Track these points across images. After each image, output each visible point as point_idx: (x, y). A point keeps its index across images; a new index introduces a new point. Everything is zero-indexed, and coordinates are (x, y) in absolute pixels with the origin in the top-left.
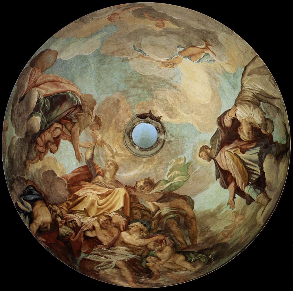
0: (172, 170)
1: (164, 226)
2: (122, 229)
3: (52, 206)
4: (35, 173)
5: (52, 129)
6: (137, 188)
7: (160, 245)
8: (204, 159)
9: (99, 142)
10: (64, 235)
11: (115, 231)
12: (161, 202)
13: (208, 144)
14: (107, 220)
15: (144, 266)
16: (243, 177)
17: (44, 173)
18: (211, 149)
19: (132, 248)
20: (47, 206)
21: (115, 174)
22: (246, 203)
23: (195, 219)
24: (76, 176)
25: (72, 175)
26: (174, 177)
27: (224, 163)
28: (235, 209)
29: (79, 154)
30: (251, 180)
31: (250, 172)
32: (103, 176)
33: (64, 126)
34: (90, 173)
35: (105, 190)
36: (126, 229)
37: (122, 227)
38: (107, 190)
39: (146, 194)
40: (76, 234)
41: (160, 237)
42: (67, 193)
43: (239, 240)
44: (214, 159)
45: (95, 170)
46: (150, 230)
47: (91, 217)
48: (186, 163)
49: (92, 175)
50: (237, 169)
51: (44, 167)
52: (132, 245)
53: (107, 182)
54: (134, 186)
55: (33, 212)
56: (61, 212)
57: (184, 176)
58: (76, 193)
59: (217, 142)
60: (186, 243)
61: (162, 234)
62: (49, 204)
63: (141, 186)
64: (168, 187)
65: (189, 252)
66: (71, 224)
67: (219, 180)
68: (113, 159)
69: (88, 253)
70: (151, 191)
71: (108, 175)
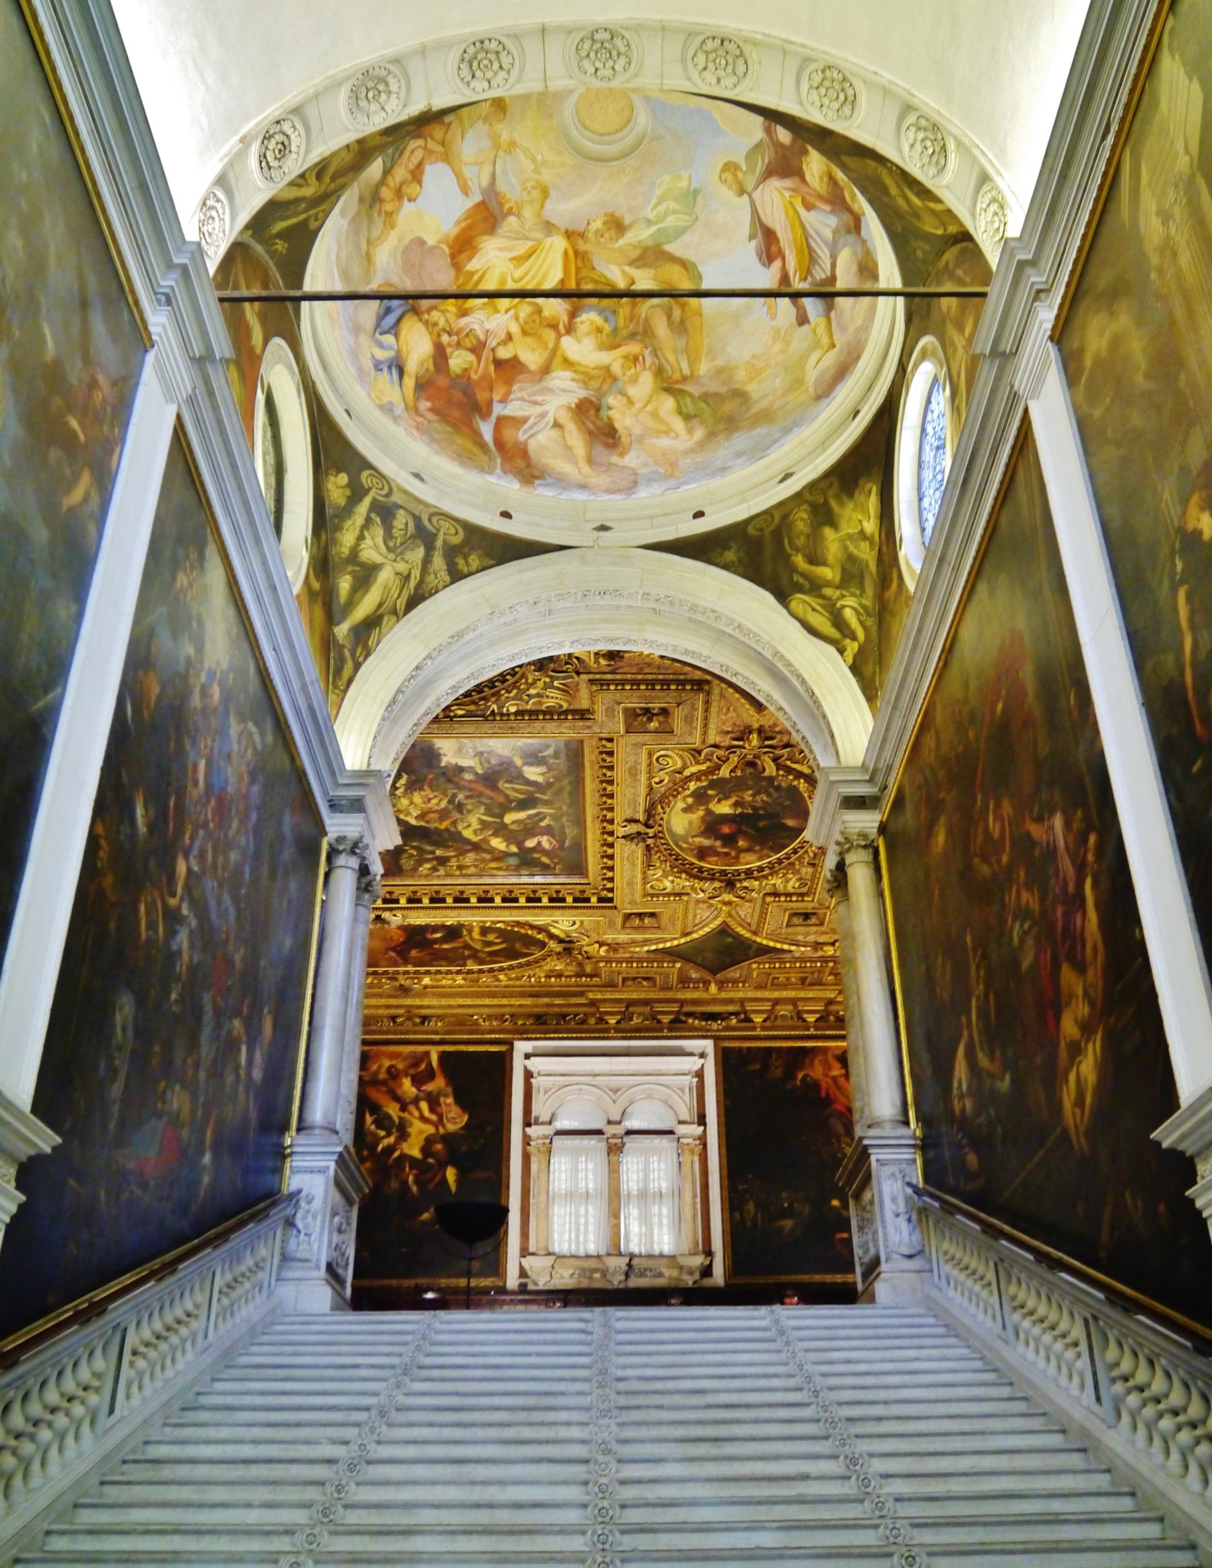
0: (661, 200)
1: (642, 321)
2: (563, 331)
5: (407, 154)
8: (730, 188)
10: (459, 371)
11: (550, 335)
12: (638, 267)
13: (740, 159)
14: (533, 313)
15: (605, 419)
16: (800, 261)
20: (421, 320)
21: (542, 206)
24: (463, 231)
25: (456, 230)
26: (666, 215)
28: (774, 323)
29: (465, 182)
30: (812, 276)
31: (810, 258)
32: (519, 215)
33: (429, 140)
35: (523, 247)
36: (570, 330)
37: (561, 327)
38: (530, 244)
40: (479, 362)
41: (634, 348)
42: (452, 272)
44: (750, 195)
45: (501, 205)
46: (615, 331)
47: (503, 311)
49: (495, 218)
50: (791, 237)
51: (401, 238)
53: (527, 227)
56: (447, 321)
58: (470, 267)
59: (760, 163)
60: (681, 369)
62: (422, 313)
63: (598, 231)
64: (653, 235)
67: (754, 242)
69: (504, 401)
70: (617, 240)
71: (528, 212)
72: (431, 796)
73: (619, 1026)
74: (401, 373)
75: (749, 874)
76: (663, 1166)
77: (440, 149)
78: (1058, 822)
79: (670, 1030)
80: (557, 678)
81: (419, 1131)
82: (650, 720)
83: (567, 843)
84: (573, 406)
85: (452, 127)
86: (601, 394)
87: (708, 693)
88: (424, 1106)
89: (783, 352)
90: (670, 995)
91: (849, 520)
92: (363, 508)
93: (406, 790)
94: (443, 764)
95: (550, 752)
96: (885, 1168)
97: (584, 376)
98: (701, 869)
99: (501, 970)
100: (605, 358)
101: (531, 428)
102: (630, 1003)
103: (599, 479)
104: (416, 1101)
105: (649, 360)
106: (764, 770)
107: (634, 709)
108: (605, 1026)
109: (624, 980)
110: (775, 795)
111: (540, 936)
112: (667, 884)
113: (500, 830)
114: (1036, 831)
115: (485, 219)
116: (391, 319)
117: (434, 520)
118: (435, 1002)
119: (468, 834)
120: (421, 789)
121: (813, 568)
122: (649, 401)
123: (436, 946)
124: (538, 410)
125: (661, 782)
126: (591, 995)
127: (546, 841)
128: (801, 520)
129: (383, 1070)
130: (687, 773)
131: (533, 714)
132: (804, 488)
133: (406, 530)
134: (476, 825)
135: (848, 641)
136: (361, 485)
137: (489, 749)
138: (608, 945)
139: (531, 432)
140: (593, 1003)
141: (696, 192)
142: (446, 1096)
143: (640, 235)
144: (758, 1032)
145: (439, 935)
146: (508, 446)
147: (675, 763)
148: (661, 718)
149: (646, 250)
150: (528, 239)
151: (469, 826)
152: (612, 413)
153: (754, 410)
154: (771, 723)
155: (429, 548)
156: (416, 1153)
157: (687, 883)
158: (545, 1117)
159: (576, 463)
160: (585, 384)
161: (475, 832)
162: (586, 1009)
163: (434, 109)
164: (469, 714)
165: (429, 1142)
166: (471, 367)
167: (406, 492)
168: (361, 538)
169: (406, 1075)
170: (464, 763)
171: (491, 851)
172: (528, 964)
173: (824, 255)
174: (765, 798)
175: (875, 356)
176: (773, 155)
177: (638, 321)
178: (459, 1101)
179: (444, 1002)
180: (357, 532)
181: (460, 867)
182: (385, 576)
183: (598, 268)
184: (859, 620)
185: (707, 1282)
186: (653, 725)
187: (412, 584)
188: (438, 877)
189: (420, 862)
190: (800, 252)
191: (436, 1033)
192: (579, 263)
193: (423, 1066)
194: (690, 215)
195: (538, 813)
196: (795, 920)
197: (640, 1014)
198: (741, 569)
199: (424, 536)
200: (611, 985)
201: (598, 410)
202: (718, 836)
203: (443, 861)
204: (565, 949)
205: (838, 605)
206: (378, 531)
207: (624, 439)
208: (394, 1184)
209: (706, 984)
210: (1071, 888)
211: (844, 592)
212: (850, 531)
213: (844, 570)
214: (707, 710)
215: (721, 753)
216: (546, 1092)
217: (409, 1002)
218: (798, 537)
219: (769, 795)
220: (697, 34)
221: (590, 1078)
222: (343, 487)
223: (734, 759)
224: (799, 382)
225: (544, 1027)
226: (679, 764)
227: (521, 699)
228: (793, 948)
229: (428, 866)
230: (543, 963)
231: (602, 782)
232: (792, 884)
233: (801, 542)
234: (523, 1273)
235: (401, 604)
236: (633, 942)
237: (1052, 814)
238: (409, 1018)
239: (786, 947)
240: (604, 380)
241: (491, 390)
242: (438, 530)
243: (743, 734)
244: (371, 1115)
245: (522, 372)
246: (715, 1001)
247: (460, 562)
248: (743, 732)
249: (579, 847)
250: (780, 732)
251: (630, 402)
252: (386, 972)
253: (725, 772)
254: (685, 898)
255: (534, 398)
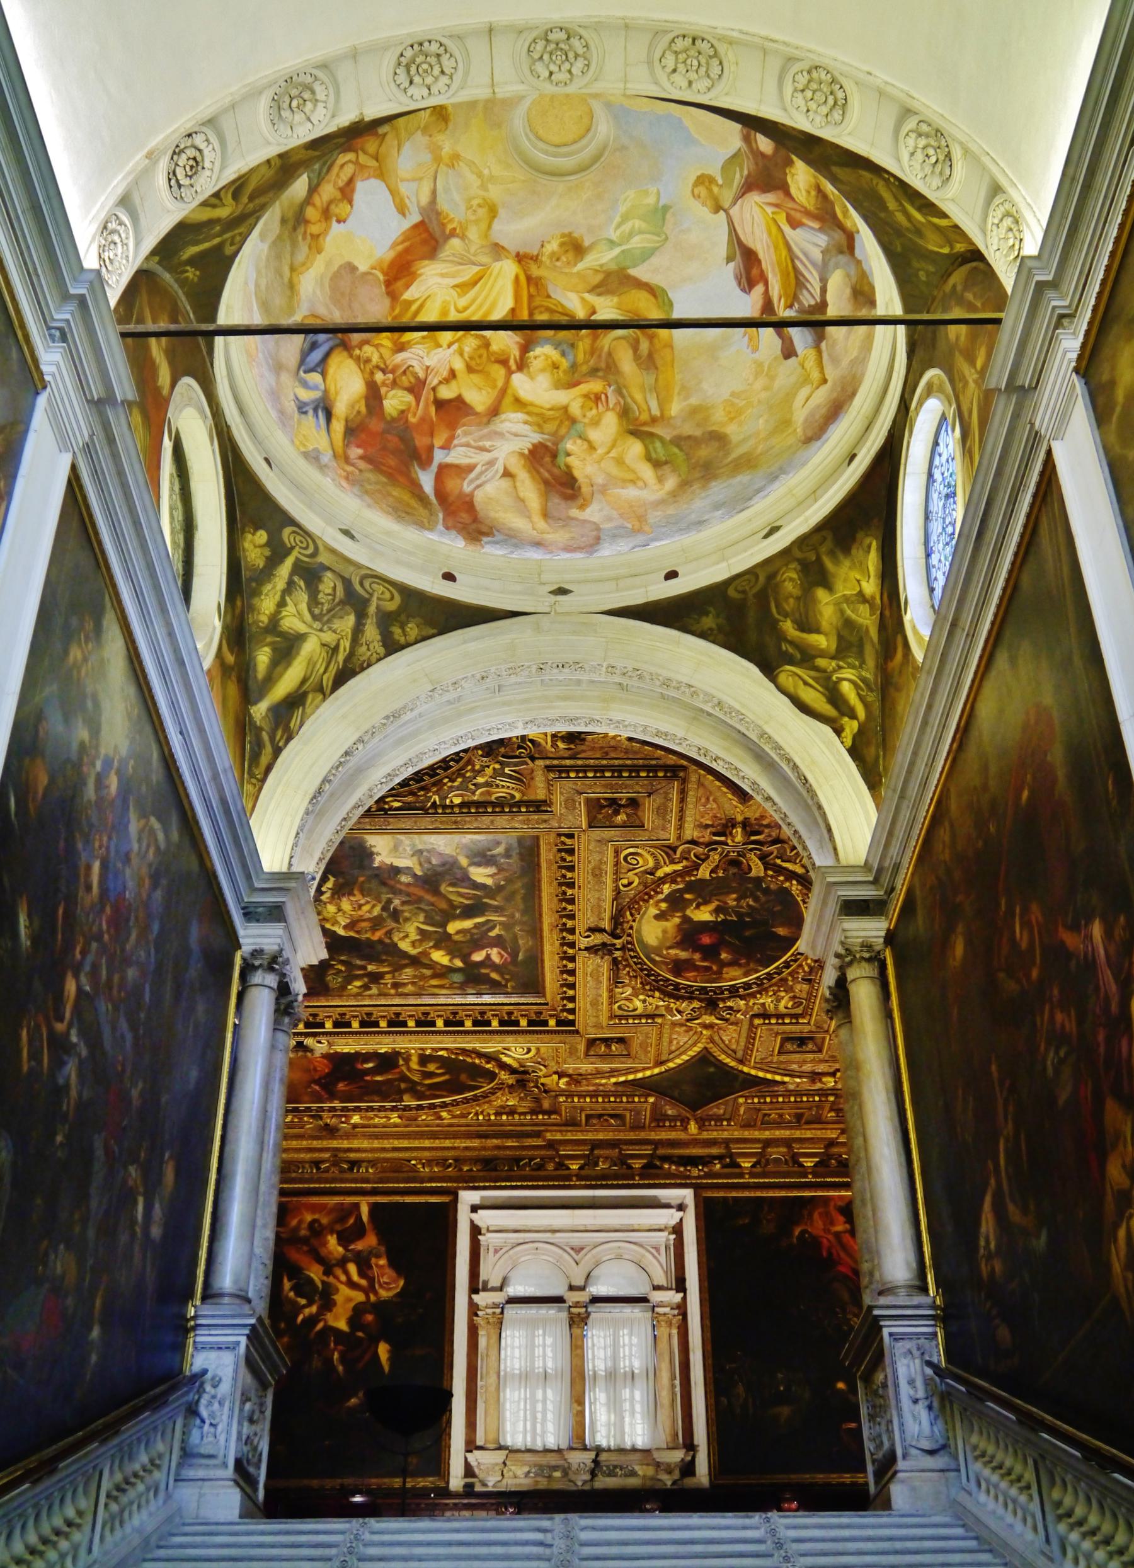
0: (625, 218)
1: (604, 355)
2: (514, 367)
3: (360, 349)
4: (314, 292)
5: (335, 169)
6: (544, 259)
7: (594, 405)
8: (704, 204)
9: (446, 160)
10: (395, 414)
11: (499, 372)
12: (599, 295)
13: (715, 171)
14: (479, 347)
15: (563, 467)
17: (331, 279)
18: (721, 186)
19: (538, 415)
20: (351, 356)
21: (489, 227)
22: (782, 351)
23: (671, 347)
24: (400, 255)
25: (391, 255)
26: (631, 235)
27: (748, 230)
28: (754, 356)
29: (402, 200)
30: (800, 303)
31: (799, 282)
32: (463, 237)
33: (360, 153)
34: (432, 236)
36: (522, 366)
37: (512, 363)
38: (476, 269)
39: (566, 274)
41: (595, 386)
42: (387, 301)
43: (752, 442)
45: (443, 226)
46: (574, 366)
47: (445, 346)
48: (661, 204)
49: (437, 242)
51: (328, 264)
52: (536, 406)
53: (472, 250)
54: (535, 253)
55: (332, 397)
56: (381, 357)
57: (654, 234)
58: (407, 296)
59: (738, 176)
60: (649, 410)
61: (600, 378)
62: (353, 348)
63: (553, 253)
64: (616, 257)
65: (652, 435)
66: (404, 378)
67: (732, 265)
68: (482, 193)
69: (446, 447)
70: (575, 265)
71: (473, 234)
72: (362, 902)
73: (583, 1172)
74: (329, 415)
75: (734, 991)
76: (635, 1340)
77: (373, 163)
78: (1097, 930)
79: (642, 1177)
80: (508, 764)
81: (347, 1297)
82: (617, 813)
83: (521, 957)
84: (526, 452)
85: (388, 137)
86: (558, 439)
87: (684, 781)
88: (352, 1268)
89: (766, 389)
90: (642, 1135)
91: (845, 580)
92: (284, 570)
93: (333, 895)
94: (376, 865)
95: (500, 850)
96: (900, 1344)
97: (539, 418)
98: (677, 986)
99: (444, 1105)
100: (562, 397)
101: (477, 478)
102: (595, 1145)
103: (559, 536)
104: (342, 1263)
105: (612, 400)
106: (750, 869)
107: (598, 799)
108: (567, 1172)
109: (588, 1117)
110: (763, 899)
111: (488, 1066)
112: (638, 1004)
113: (443, 941)
114: (1071, 940)
115: (424, 242)
116: (317, 355)
117: (367, 584)
118: (365, 1144)
119: (404, 946)
120: (351, 894)
121: (805, 635)
122: (613, 446)
123: (368, 1078)
124: (487, 457)
125: (630, 884)
126: (549, 1136)
127: (495, 955)
128: (790, 580)
129: (305, 1226)
130: (660, 873)
131: (481, 806)
132: (793, 543)
133: (334, 595)
134: (414, 936)
135: (846, 719)
136: (283, 544)
137: (429, 847)
138: (569, 1076)
139: (478, 482)
140: (551, 1145)
141: (666, 209)
142: (378, 1257)
143: (601, 258)
144: (747, 1180)
145: (370, 1065)
146: (451, 499)
147: (646, 862)
148: (629, 811)
149: (608, 274)
150: (474, 264)
151: (407, 936)
152: (569, 460)
153: (734, 455)
154: (757, 815)
155: (361, 616)
156: (342, 1325)
157: (662, 1003)
158: (495, 1282)
159: (529, 517)
160: (540, 428)
161: (413, 944)
162: (543, 1152)
163: (367, 119)
164: (407, 807)
165: (358, 1311)
166: (408, 410)
167: (333, 551)
168: (282, 604)
169: (332, 1233)
170: (401, 863)
171: (433, 965)
172: (475, 1099)
173: (813, 279)
174: (751, 903)
175: (871, 395)
176: (752, 167)
177: (600, 356)
178: (392, 1264)
179: (376, 1144)
180: (278, 597)
181: (396, 985)
182: (310, 647)
183: (553, 296)
184: (858, 694)
185: (689, 1482)
186: (621, 818)
187: (341, 657)
188: (370, 996)
189: (349, 979)
190: (785, 275)
191: (367, 1181)
192: (532, 290)
193: (351, 1221)
194: (658, 235)
195: (488, 921)
196: (789, 1046)
197: (606, 1158)
198: (721, 637)
199: (354, 601)
200: (572, 1123)
201: (554, 456)
202: (697, 947)
203: (376, 978)
204: (518, 1081)
205: (834, 678)
206: (302, 597)
207: (585, 490)
208: (316, 1363)
209: (685, 1122)
210: (1114, 1007)
211: (841, 663)
212: (847, 592)
213: (840, 638)
214: (682, 800)
215: (700, 850)
216: (496, 1251)
217: (335, 1144)
218: (787, 599)
219: (756, 900)
220: (666, 32)
221: (549, 1235)
222: (261, 546)
223: (715, 857)
224: (786, 423)
225: (494, 1174)
226: (651, 864)
227: (467, 789)
228: (787, 1079)
229: (358, 983)
230: (493, 1098)
231: (561, 884)
232: (785, 1004)
233: (790, 605)
234: (469, 1471)
235: (328, 680)
236: (599, 1073)
237: (1089, 921)
238: (336, 1163)
239: (778, 1078)
240: (562, 422)
241: (432, 435)
242: (371, 595)
243: (726, 827)
244: (289, 1280)
245: (467, 415)
246: (695, 1142)
247: (397, 631)
248: (725, 826)
249: (535, 960)
250: (768, 826)
251: (592, 447)
252: (308, 1109)
253: (704, 872)
254: (659, 1020)
255: (481, 444)
